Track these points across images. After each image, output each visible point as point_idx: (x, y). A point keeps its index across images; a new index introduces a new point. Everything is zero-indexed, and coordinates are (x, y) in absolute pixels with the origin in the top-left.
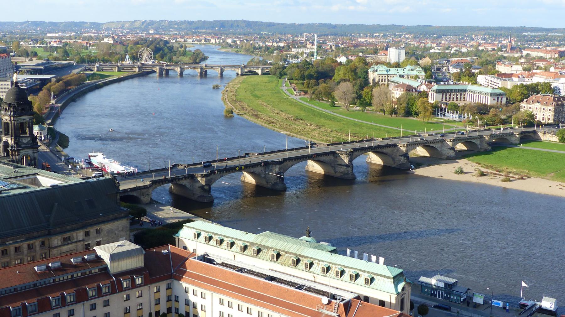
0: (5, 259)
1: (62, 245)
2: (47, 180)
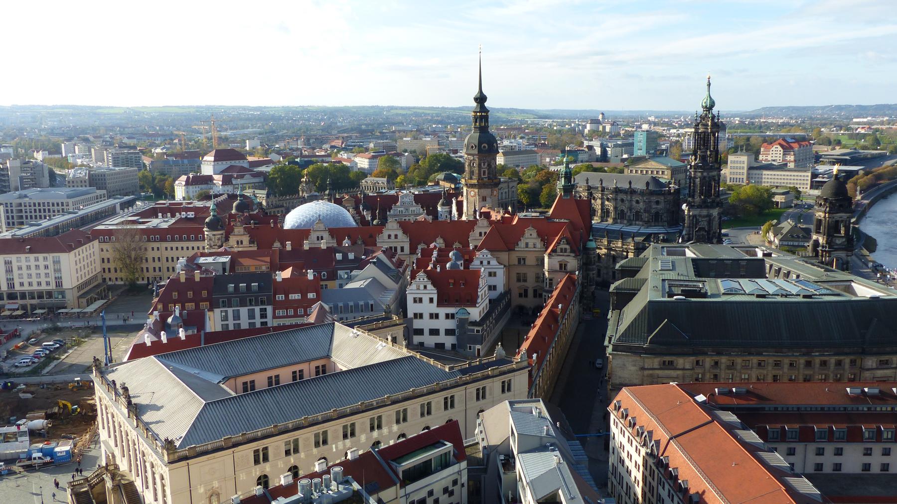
0: (808, 372)
1: (877, 369)
2: (864, 291)
